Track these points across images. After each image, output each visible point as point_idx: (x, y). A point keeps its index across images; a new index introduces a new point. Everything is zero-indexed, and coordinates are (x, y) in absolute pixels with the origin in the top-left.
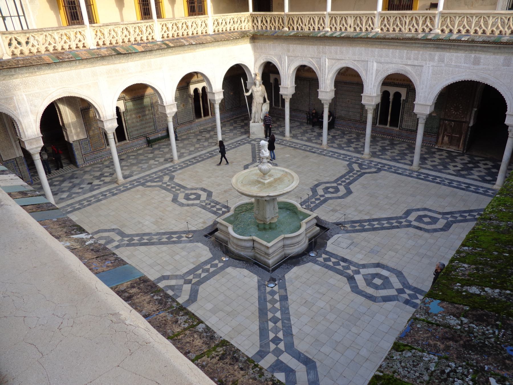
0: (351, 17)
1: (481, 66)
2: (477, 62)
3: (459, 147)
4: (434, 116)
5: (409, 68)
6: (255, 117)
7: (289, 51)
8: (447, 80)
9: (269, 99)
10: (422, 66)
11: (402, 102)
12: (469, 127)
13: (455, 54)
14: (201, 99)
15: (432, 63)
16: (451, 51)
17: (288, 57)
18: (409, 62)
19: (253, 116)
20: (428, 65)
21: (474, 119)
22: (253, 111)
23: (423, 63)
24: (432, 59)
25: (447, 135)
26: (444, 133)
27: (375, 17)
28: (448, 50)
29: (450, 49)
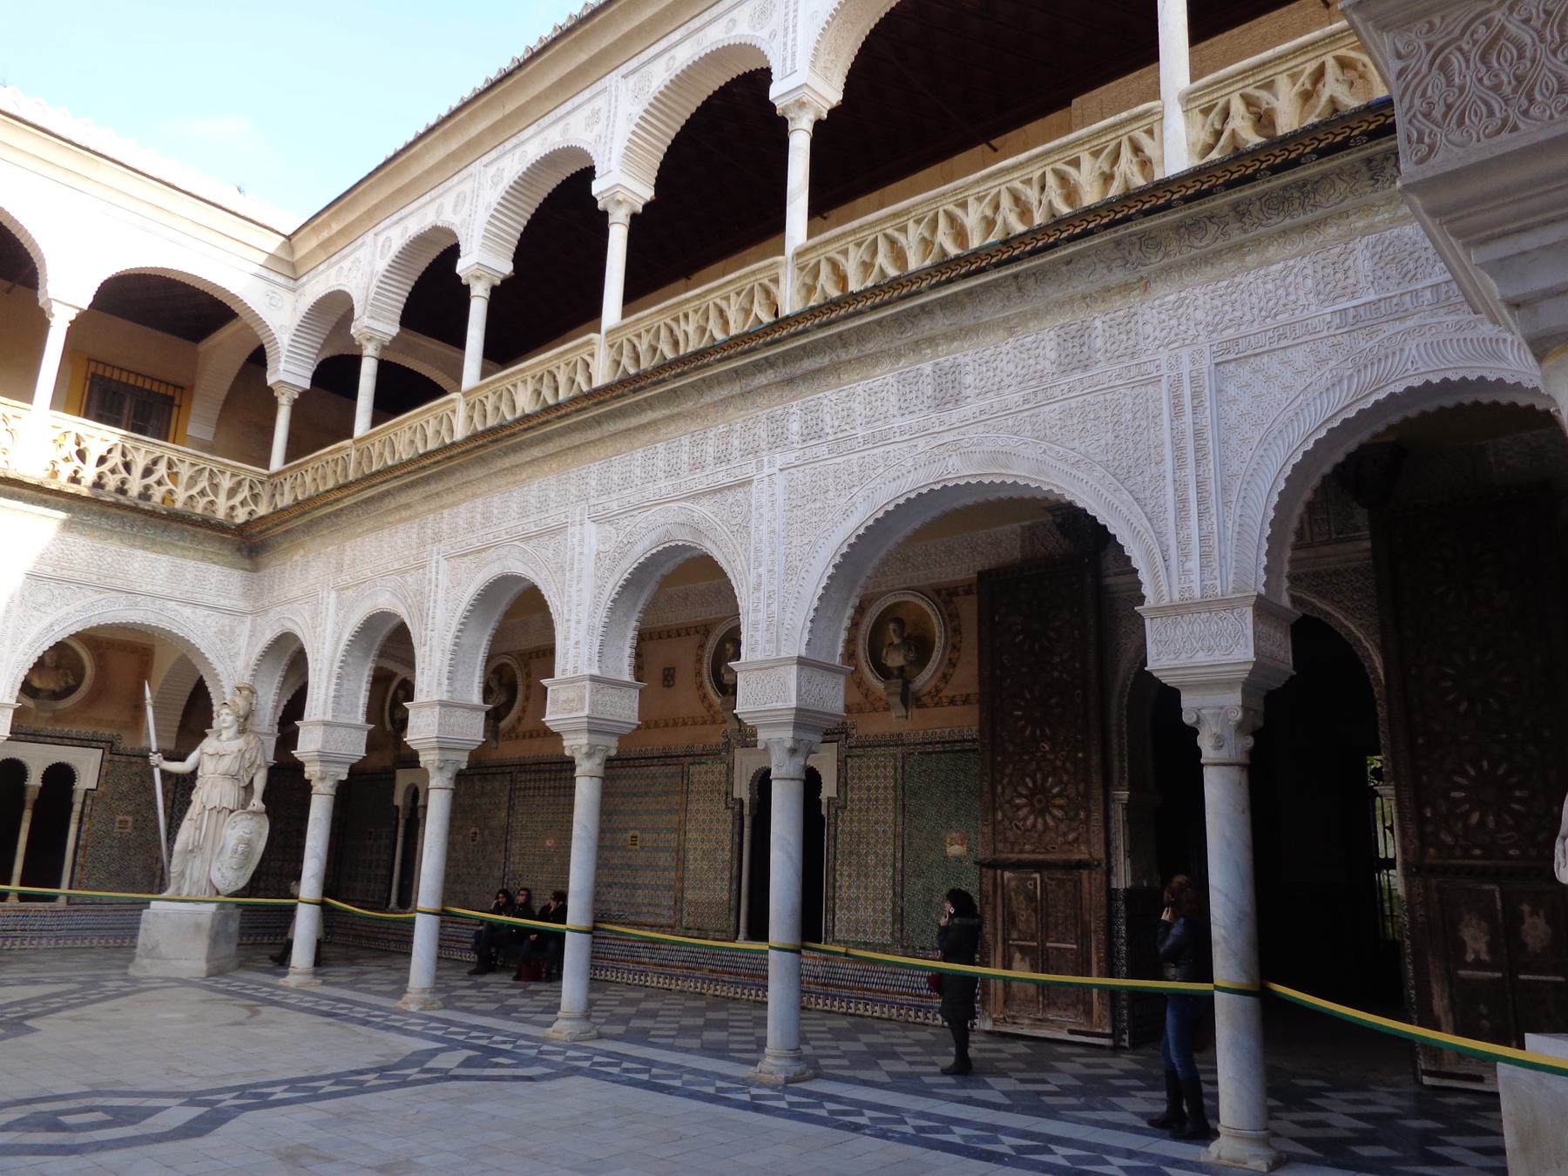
0: (525, 382)
1: (969, 409)
2: (947, 395)
3: (1088, 1013)
4: (959, 859)
5: (703, 510)
6: (182, 874)
7: (339, 568)
8: (846, 514)
9: (265, 799)
10: (746, 483)
11: (824, 812)
12: (1111, 893)
13: (860, 388)
14: (27, 816)
15: (780, 459)
16: (845, 377)
17: (340, 590)
18: (702, 481)
19: (175, 868)
20: (767, 471)
21: (1131, 852)
22: (178, 847)
23: (750, 469)
24: (778, 440)
25: (1022, 949)
26: (1005, 941)
27: (592, 355)
28: (833, 380)
29: (835, 368)
